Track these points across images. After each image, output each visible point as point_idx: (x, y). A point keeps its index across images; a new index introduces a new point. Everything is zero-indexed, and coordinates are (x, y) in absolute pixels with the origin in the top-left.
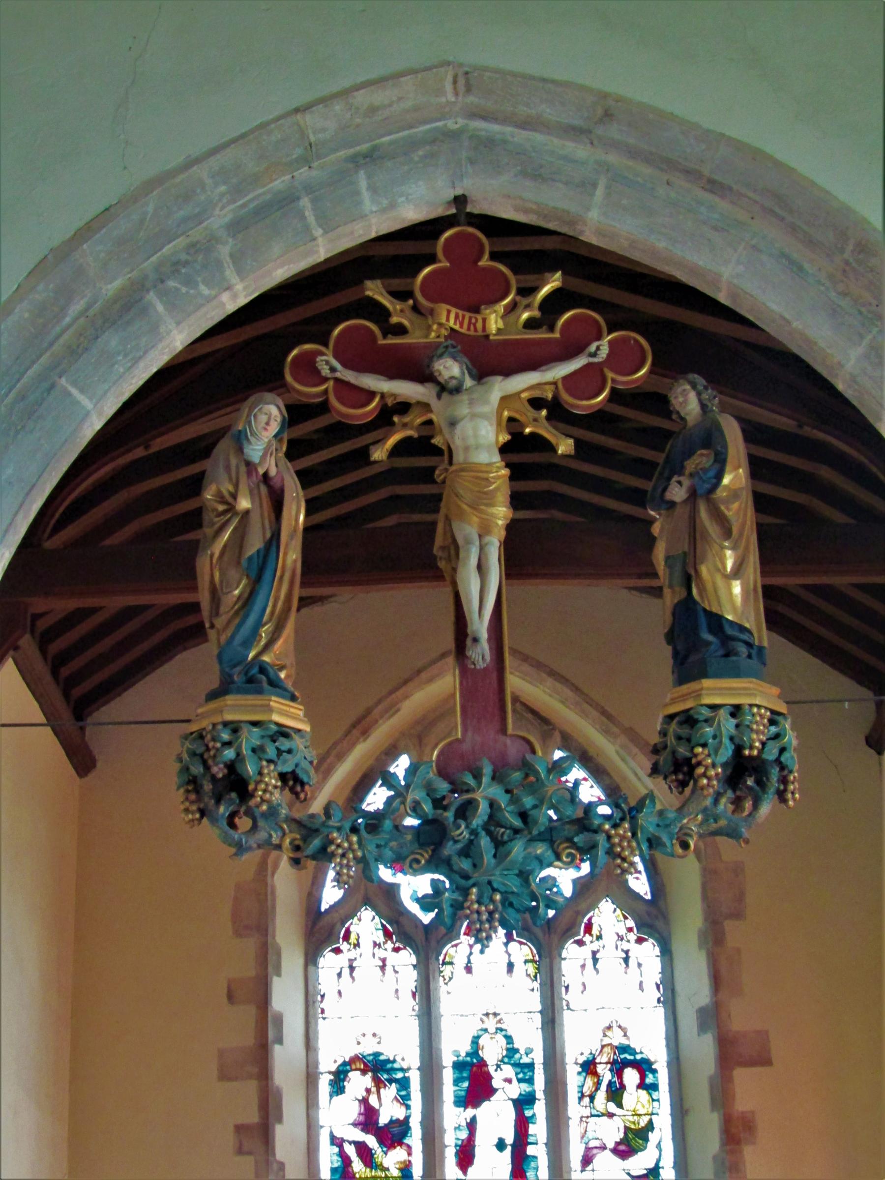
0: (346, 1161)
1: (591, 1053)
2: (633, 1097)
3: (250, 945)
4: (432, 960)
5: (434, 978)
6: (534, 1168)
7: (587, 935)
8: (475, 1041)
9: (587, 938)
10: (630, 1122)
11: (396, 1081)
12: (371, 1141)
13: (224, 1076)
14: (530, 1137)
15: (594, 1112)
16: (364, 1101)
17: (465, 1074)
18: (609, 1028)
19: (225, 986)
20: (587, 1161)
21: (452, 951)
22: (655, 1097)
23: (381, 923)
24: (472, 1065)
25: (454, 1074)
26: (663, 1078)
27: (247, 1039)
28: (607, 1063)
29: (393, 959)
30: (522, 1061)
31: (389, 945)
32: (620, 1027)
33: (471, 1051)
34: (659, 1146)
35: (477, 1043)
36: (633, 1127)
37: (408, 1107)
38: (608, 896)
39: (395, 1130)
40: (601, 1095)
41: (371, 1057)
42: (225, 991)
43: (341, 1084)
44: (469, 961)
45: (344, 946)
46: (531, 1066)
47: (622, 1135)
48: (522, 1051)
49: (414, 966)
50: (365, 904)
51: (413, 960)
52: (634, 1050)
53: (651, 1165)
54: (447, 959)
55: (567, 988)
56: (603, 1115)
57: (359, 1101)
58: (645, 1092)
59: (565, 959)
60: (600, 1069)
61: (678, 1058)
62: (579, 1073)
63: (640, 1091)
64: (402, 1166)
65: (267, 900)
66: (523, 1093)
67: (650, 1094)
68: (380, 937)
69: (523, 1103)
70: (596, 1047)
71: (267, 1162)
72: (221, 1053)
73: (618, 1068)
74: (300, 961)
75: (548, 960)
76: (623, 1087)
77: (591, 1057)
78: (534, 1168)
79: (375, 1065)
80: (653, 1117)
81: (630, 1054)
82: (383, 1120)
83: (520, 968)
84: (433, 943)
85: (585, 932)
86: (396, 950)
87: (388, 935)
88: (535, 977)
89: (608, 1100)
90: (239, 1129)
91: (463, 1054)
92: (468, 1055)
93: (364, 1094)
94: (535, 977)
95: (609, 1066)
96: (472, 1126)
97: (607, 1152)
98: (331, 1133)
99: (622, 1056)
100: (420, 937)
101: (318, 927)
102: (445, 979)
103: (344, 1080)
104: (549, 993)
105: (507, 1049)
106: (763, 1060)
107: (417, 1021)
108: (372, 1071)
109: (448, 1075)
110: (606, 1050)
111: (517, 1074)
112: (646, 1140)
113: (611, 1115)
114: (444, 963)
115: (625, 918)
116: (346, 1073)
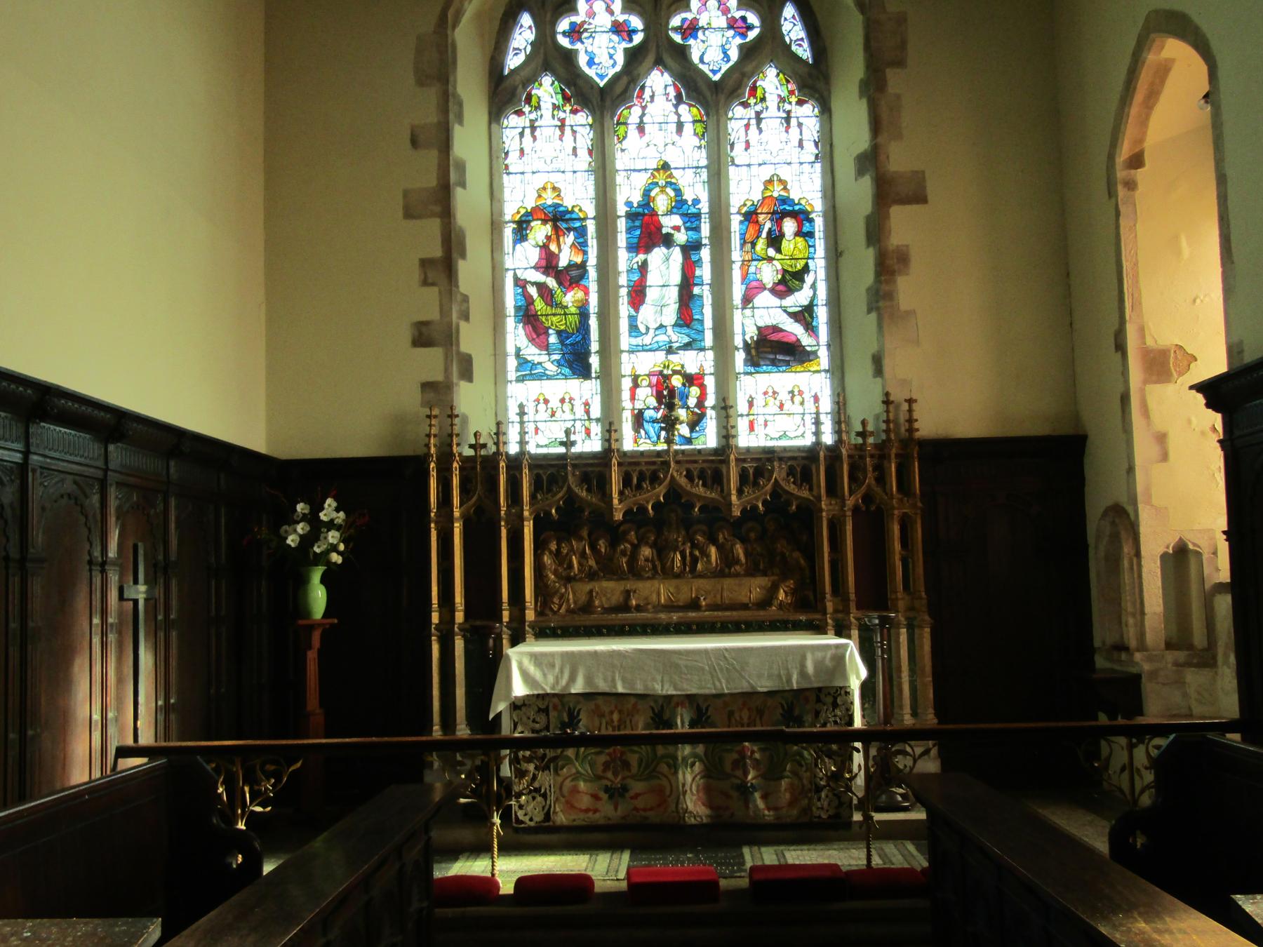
0: (529, 301)
1: (753, 205)
2: (791, 244)
3: (431, 95)
4: (607, 118)
5: (609, 135)
6: (700, 306)
7: (752, 98)
8: (646, 193)
9: (752, 101)
10: (789, 265)
11: (575, 229)
12: (551, 282)
13: (409, 214)
14: (696, 279)
15: (755, 257)
16: (545, 247)
17: (638, 223)
18: (770, 181)
19: (409, 132)
20: (747, 300)
21: (625, 112)
22: (810, 244)
23: (561, 88)
24: (643, 215)
25: (626, 223)
26: (819, 224)
27: (430, 180)
28: (768, 213)
29: (571, 120)
30: (689, 212)
31: (568, 108)
32: (780, 181)
33: (644, 203)
34: (813, 286)
35: (649, 196)
36: (790, 269)
37: (585, 253)
38: (772, 61)
39: (574, 273)
40: (761, 244)
41: (552, 209)
42: (409, 136)
43: (524, 232)
44: (642, 121)
45: (527, 109)
46: (698, 216)
47: (780, 277)
48: (690, 203)
49: (591, 126)
50: (546, 70)
51: (590, 120)
52: (793, 200)
53: (806, 303)
54: (621, 120)
55: (732, 145)
56: (764, 259)
57: (540, 247)
58: (802, 239)
59: (731, 119)
60: (761, 218)
61: (834, 207)
62: (741, 222)
63: (797, 238)
64: (580, 305)
65: (447, 51)
66: (690, 240)
67: (806, 241)
68: (559, 100)
69: (690, 249)
70: (757, 196)
71: (450, 292)
72: (406, 194)
73: (779, 217)
74: (485, 118)
75: (715, 117)
76: (782, 235)
77: (753, 209)
78: (700, 306)
79: (555, 216)
80: (809, 261)
81: (790, 206)
82: (563, 263)
83: (688, 128)
84: (608, 103)
85: (750, 95)
86: (574, 112)
87: (566, 99)
88: (703, 135)
89: (768, 247)
90: (425, 263)
91: (635, 205)
92: (639, 206)
93: (545, 241)
94: (703, 135)
95: (770, 215)
96: (643, 268)
97: (766, 292)
98: (515, 274)
99: (782, 207)
100: (595, 99)
101: (500, 89)
102: (619, 138)
103: (526, 229)
104: (716, 148)
105: (676, 201)
106: (919, 197)
107: (592, 177)
108: (551, 220)
109: (622, 224)
110: (767, 201)
111: (684, 223)
112: (803, 281)
113: (770, 259)
114: (618, 124)
115: (788, 82)
116: (528, 222)
